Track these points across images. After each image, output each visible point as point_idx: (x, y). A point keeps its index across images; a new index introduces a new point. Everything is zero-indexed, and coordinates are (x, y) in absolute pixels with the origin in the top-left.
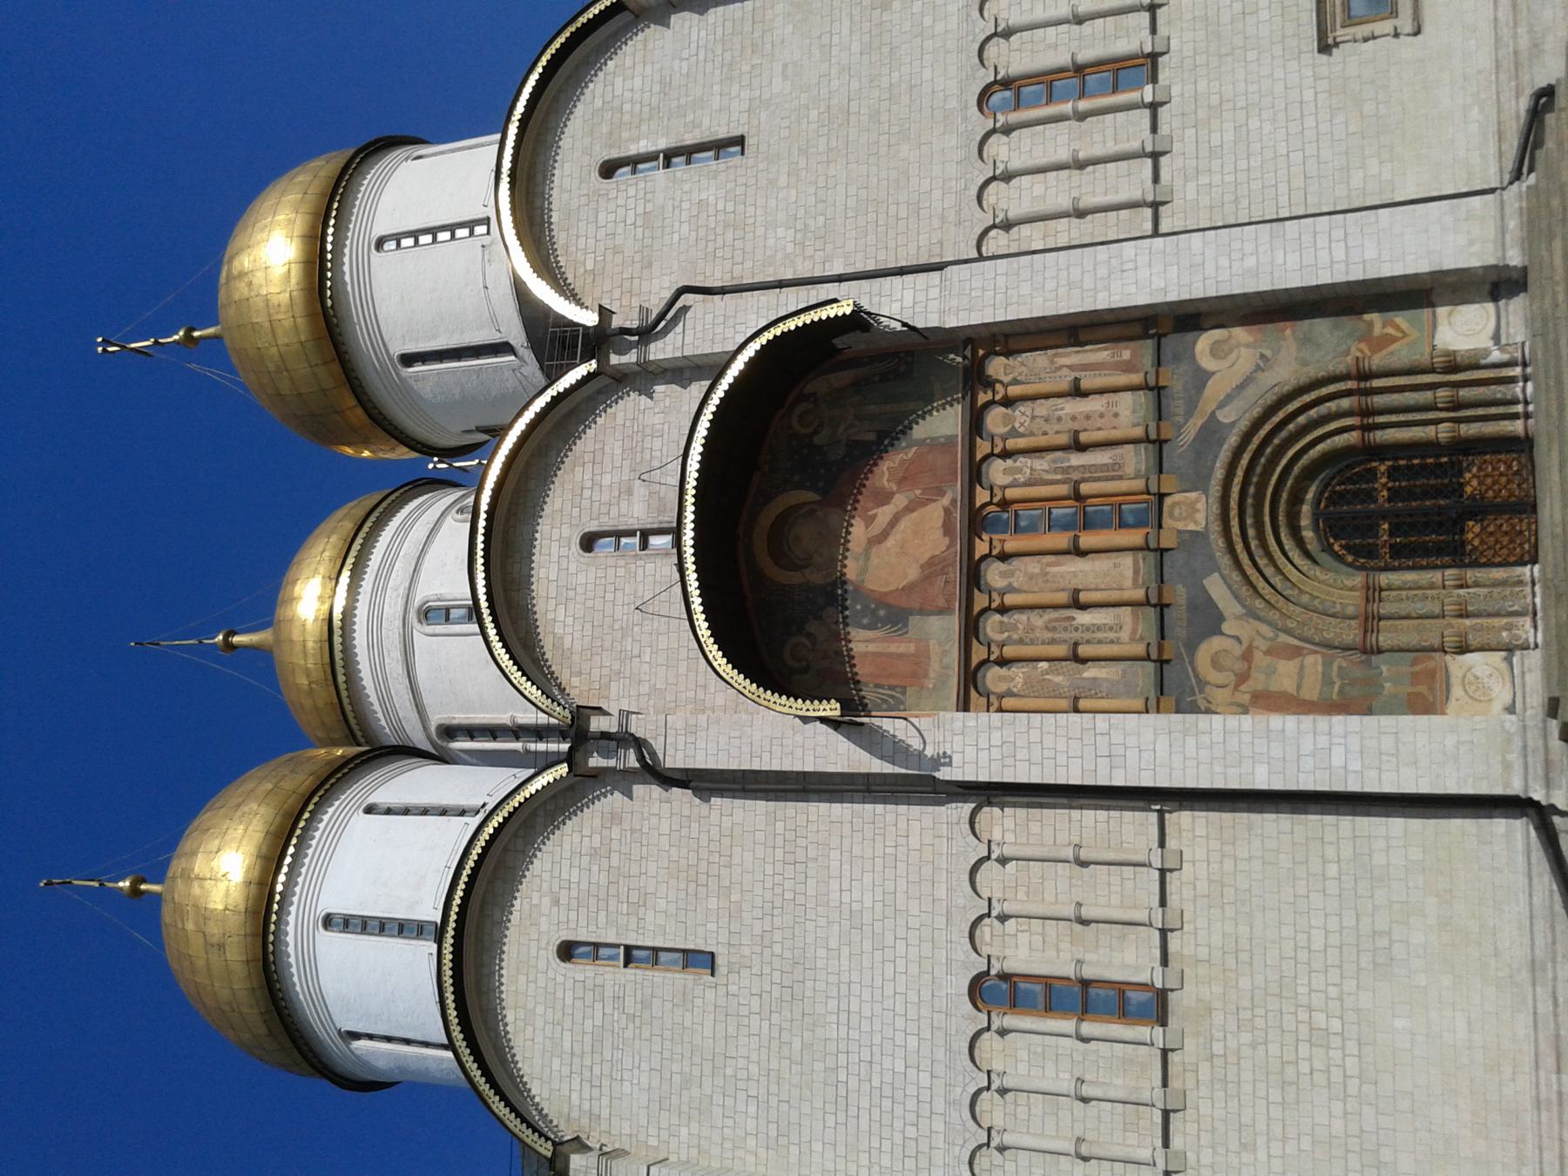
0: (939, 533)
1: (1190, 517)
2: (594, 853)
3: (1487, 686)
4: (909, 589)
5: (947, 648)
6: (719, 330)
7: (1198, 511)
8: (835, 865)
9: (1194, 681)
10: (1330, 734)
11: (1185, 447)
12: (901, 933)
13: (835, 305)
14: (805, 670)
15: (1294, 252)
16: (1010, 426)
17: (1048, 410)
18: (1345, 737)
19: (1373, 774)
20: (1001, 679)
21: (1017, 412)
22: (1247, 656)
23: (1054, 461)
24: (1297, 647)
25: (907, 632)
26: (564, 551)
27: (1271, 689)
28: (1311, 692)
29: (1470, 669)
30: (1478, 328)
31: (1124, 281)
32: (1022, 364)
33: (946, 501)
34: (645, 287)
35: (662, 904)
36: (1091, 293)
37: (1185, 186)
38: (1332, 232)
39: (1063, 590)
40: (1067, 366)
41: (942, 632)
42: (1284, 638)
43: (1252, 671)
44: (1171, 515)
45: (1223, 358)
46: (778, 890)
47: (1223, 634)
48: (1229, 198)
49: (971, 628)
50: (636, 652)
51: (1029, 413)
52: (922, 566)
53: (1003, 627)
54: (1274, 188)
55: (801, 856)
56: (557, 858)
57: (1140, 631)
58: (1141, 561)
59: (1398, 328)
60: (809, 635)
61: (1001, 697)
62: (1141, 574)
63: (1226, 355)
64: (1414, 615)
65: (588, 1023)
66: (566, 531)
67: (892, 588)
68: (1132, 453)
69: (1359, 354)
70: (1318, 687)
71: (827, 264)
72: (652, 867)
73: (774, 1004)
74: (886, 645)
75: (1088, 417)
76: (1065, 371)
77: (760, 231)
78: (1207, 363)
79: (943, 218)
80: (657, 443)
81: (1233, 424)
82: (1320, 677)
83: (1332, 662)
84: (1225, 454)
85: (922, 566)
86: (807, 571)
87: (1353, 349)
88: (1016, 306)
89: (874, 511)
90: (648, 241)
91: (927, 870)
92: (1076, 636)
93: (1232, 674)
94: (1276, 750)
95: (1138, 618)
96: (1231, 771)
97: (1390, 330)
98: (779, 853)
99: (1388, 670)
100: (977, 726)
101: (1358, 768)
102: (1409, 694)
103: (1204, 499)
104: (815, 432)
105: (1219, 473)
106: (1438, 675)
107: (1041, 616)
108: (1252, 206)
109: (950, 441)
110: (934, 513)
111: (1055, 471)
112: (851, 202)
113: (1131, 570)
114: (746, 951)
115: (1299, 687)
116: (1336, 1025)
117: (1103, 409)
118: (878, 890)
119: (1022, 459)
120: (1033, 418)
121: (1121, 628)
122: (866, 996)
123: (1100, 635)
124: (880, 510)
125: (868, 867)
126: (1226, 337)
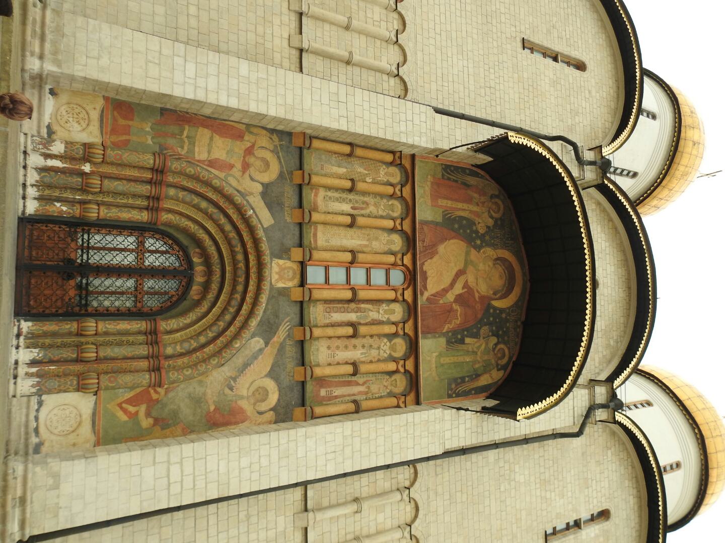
0: (429, 274)
1: (282, 269)
2: (577, 114)
3: (70, 115)
4: (443, 239)
5: (422, 199)
7: (277, 273)
8: (472, 82)
9: (280, 154)
11: (285, 322)
12: (438, 37)
13: (526, 415)
15: (211, 472)
16: (392, 343)
17: (371, 353)
19: (165, 51)
21: (388, 353)
22: (246, 166)
24: (211, 167)
25: (443, 212)
27: (230, 140)
28: (203, 134)
30: (55, 411)
32: (386, 387)
33: (426, 294)
35: (547, 81)
36: (355, 434)
37: (285, 528)
38: (179, 490)
40: (359, 385)
42: (222, 175)
44: (294, 273)
46: (497, 75)
47: (262, 184)
48: (254, 519)
49: (410, 209)
51: (382, 352)
52: (437, 253)
54: (220, 530)
57: (313, 195)
58: (312, 242)
59: (125, 411)
60: (491, 217)
62: (312, 233)
63: (257, 390)
64: (125, 182)
65: (571, 29)
67: (452, 241)
68: (319, 319)
69: (159, 389)
70: (198, 136)
71: (497, 458)
73: (495, 16)
74: (454, 206)
75: (346, 347)
77: (532, 479)
78: (270, 385)
81: (253, 336)
82: (197, 144)
83: (187, 152)
84: (260, 311)
85: (437, 253)
86: (495, 257)
88: (402, 424)
89: (464, 291)
92: (351, 196)
93: (256, 154)
94: (234, 83)
95: (314, 203)
96: (265, 76)
97: (132, 409)
99: (147, 140)
100: (414, 136)
101: (176, 58)
102: (132, 120)
103: (273, 281)
104: (496, 345)
105: (264, 298)
106: (109, 129)
107: (371, 212)
108: (237, 513)
110: (433, 286)
111: (365, 311)
112: (487, 503)
113: (318, 237)
114: (509, 46)
115: (211, 139)
117: (337, 352)
118: (450, 63)
119: (385, 320)
120: (379, 348)
121: (324, 198)
122: (453, 8)
123: (337, 195)
124: (461, 291)
126: (258, 404)
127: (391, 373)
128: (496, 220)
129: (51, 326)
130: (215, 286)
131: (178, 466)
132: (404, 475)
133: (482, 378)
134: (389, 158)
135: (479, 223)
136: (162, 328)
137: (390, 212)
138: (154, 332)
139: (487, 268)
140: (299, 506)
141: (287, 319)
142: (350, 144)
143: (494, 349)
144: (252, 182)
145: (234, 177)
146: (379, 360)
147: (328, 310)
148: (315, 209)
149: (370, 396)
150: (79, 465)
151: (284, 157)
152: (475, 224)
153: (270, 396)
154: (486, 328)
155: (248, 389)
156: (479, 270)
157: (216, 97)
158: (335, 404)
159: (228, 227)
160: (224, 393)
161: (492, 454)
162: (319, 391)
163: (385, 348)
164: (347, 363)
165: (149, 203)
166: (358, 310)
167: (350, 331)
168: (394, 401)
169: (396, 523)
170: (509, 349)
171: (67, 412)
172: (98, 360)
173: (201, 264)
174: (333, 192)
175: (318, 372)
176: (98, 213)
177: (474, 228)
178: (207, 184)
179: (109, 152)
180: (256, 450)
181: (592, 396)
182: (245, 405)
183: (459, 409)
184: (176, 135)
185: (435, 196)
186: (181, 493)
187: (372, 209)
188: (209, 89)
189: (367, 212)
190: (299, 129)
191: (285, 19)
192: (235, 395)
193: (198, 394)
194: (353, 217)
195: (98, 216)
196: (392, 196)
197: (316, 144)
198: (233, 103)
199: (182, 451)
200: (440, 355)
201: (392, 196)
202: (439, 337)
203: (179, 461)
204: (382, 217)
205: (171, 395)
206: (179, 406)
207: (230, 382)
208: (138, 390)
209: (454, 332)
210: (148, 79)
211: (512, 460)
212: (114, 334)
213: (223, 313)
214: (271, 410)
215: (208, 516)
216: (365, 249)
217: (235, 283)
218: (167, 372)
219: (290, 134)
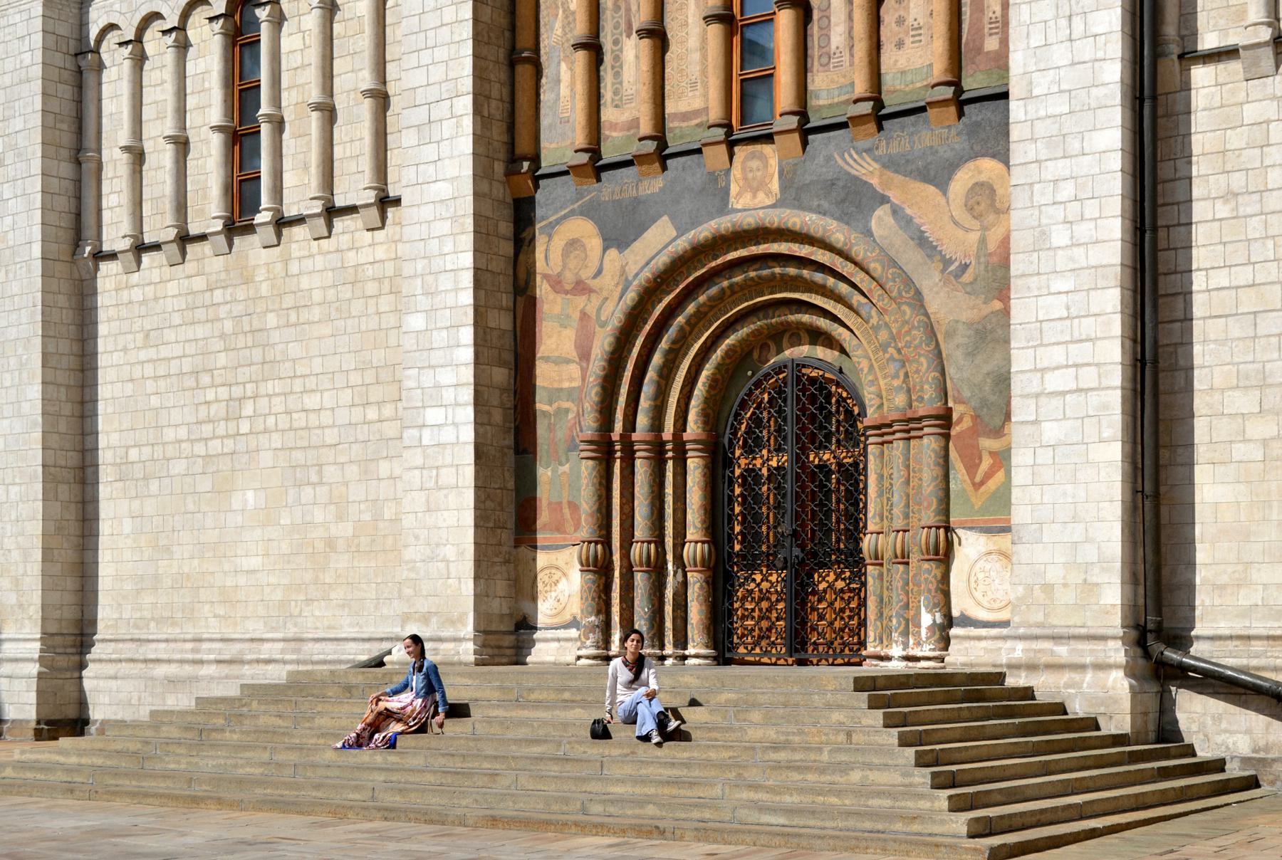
3: (548, 595)
7: (754, 196)
9: (552, 219)
15: (1068, 308)
18: (453, 423)
22: (581, 288)
24: (589, 355)
29: (565, 574)
30: (978, 595)
31: (1052, 23)
43: (564, 296)
44: (753, 156)
45: (966, 206)
47: (605, 249)
57: (614, 134)
59: (989, 475)
62: (684, 125)
63: (971, 210)
68: (842, 80)
69: (955, 417)
78: (962, 180)
81: (868, 233)
82: (556, 385)
93: (559, 269)
95: (628, 130)
96: (419, 281)
97: (986, 463)
101: (425, 442)
103: (769, 202)
108: (1217, 224)
113: (688, 109)
116: (245, 427)
117: (910, 21)
121: (616, 106)
131: (1048, 376)
136: (876, 416)
141: (840, 162)
144: (604, 272)
145: (599, 309)
147: (824, 60)
151: (556, 212)
153: (983, 178)
155: (967, 230)
157: (463, 368)
160: (971, 283)
162: (988, 52)
165: (670, 458)
171: (981, 576)
174: (605, 86)
176: (696, 542)
180: (1040, 212)
184: (550, 424)
186: (1097, 365)
188: (454, 381)
190: (499, 191)
192: (978, 257)
193: (969, 337)
195: (703, 542)
199: (1022, 372)
203: (1039, 375)
205: (966, 393)
206: (988, 374)
207: (950, 273)
210: (460, 485)
213: (839, 299)
215: (1209, 291)
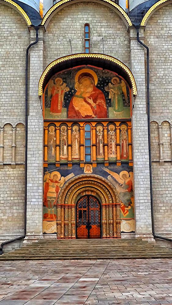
0: (86, 114)
1: (87, 170)
2: (11, 32)
4: (73, 108)
5: (59, 117)
6: (137, 58)
10: (39, 198)
13: (136, 90)
14: (55, 84)
19: (30, 207)
20: (52, 130)
22: (56, 182)
23: (101, 140)
26: (85, 19)
27: (49, 187)
28: (49, 195)
30: (125, 229)
33: (93, 116)
34: (152, 37)
39: (72, 142)
41: (62, 115)
42: (60, 189)
44: (88, 166)
47: (61, 177)
49: (64, 123)
50: (59, 40)
51: (113, 134)
52: (78, 110)
53: (64, 130)
55: (12, 84)
56: (10, 22)
59: (126, 213)
60: (63, 84)
61: (48, 130)
63: (123, 177)
66: (90, 19)
68: (102, 157)
69: (121, 205)
72: (8, 47)
75: (111, 148)
76: (122, 142)
77: (163, 67)
78: (121, 173)
79: (162, 113)
80: (111, 42)
85: (78, 110)
87: (122, 204)
90: (164, 37)
91: (9, 114)
97: (126, 211)
98: (12, 79)
100: (40, 125)
102: (48, 214)
104: (112, 84)
105: (96, 176)
109: (107, 116)
110: (90, 113)
111: (99, 141)
112: (168, 90)
115: (50, 192)
120: (112, 135)
125: (10, 100)
127: (120, 131)
128: (64, 82)
129: (104, 230)
130: (92, 189)
132: (154, 126)
133: (124, 91)
134: (46, 131)
135: (65, 90)
137: (65, 130)
138: (106, 206)
139: (82, 87)
140: (158, 164)
142: (44, 147)
143: (113, 85)
146: (116, 135)
148: (67, 159)
149: (127, 139)
150: (137, 223)
152: (66, 92)
154: (105, 88)
156: (84, 92)
158: (129, 152)
159: (75, 186)
161: (151, 87)
163: (112, 133)
164: (116, 147)
166: (99, 143)
167: (106, 147)
168: (129, 130)
169: (169, 129)
170: (113, 77)
172: (113, 219)
173: (85, 193)
175: (119, 158)
177: (68, 93)
178: (63, 193)
179: (58, 219)
181: (134, 39)
182: (126, 182)
183: (133, 107)
185: (57, 111)
187: (65, 138)
189: (66, 139)
191: (6, 170)
194: (68, 146)
196: (60, 130)
197: (46, 159)
198: (41, 188)
200: (115, 110)
201: (60, 130)
202: (108, 110)
204: (67, 134)
205: (123, 202)
208: (121, 210)
209: (107, 103)
211: (155, 77)
212: (106, 216)
214: (129, 173)
216: (79, 141)
217: (92, 184)
218: (117, 203)
219: (44, 168)
